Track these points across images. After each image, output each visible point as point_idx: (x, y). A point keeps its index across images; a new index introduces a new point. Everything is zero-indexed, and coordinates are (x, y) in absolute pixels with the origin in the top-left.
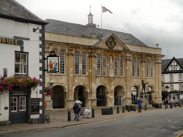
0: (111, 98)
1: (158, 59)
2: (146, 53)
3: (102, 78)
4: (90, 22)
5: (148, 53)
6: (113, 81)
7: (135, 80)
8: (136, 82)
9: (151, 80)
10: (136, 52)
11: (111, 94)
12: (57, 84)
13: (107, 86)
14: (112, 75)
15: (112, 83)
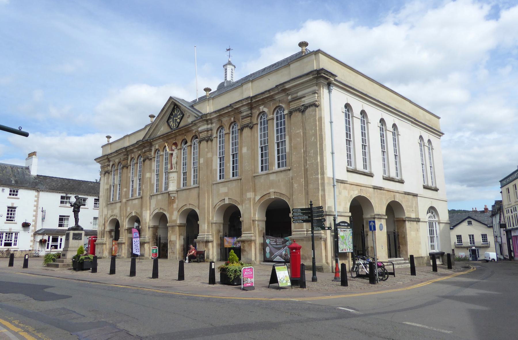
0: (172, 240)
1: (300, 94)
2: (241, 101)
3: (160, 197)
4: (229, 79)
5: (247, 99)
6: (176, 201)
7: (223, 190)
8: (226, 194)
9: (273, 177)
10: (215, 112)
11: (173, 231)
12: (115, 217)
13: (166, 213)
14: (172, 187)
15: (175, 206)
